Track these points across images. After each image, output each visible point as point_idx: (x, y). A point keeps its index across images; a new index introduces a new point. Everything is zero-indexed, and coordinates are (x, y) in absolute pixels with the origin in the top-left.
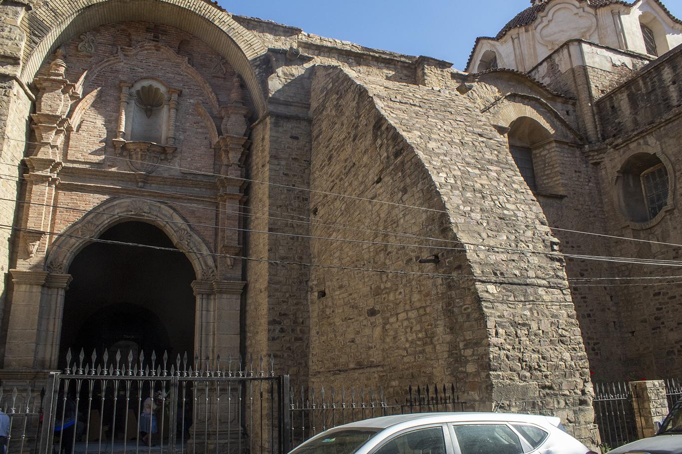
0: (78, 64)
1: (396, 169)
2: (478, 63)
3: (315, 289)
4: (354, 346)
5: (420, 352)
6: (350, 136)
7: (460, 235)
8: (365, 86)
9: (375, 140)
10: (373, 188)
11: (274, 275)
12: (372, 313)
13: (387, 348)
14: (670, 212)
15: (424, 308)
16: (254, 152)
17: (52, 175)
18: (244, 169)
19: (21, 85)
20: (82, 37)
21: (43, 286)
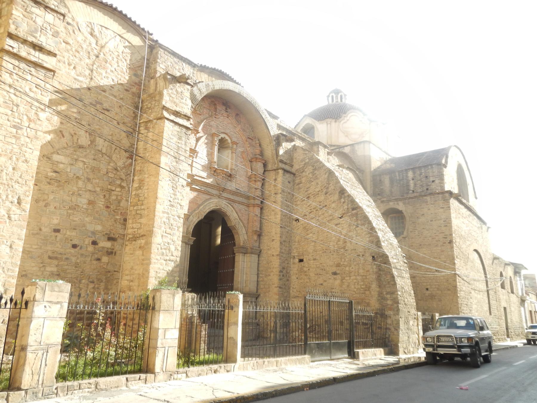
1: (353, 215)
2: (301, 128)
4: (322, 286)
5: (363, 293)
7: (385, 251)
9: (340, 198)
12: (335, 274)
14: (404, 238)
15: (366, 276)
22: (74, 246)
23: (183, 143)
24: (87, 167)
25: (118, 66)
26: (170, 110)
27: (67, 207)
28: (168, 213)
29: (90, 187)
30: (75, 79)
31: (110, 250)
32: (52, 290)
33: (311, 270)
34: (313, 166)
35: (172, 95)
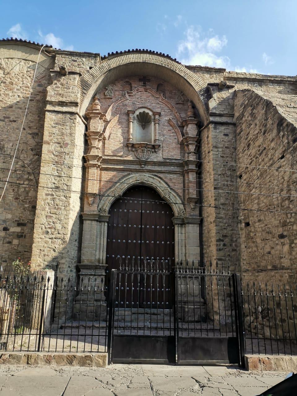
0: (106, 103)
3: (243, 221)
6: (261, 132)
8: (270, 100)
10: (279, 162)
11: (218, 214)
12: (282, 236)
13: (293, 258)
16: (203, 145)
17: (98, 163)
18: (197, 155)
19: (80, 117)
20: (106, 88)
21: (97, 221)
23: (68, 127)
25: (23, 84)
26: (54, 103)
28: (52, 195)
33: (257, 235)
35: (57, 89)
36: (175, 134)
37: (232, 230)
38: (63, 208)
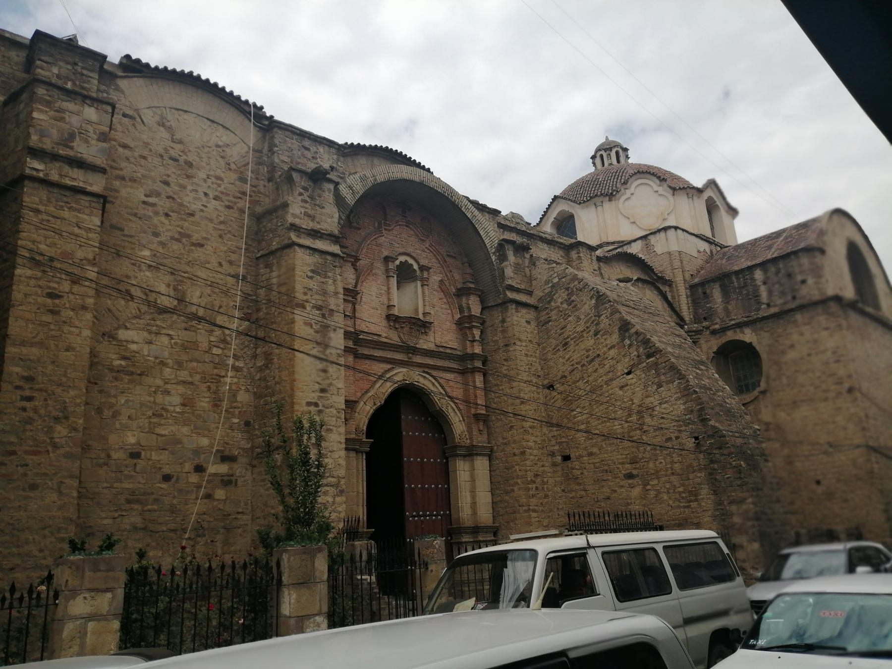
1: (649, 368)
2: (552, 219)
4: (609, 502)
9: (623, 340)
14: (763, 392)
22: (167, 478)
23: (330, 281)
24: (176, 343)
27: (150, 413)
28: (316, 405)
29: (184, 375)
30: (144, 203)
31: (226, 478)
32: (96, 569)
34: (567, 289)
36: (447, 306)
37: (543, 466)
38: (334, 428)
